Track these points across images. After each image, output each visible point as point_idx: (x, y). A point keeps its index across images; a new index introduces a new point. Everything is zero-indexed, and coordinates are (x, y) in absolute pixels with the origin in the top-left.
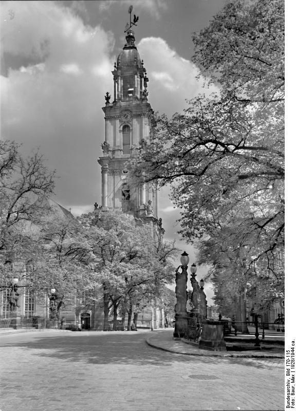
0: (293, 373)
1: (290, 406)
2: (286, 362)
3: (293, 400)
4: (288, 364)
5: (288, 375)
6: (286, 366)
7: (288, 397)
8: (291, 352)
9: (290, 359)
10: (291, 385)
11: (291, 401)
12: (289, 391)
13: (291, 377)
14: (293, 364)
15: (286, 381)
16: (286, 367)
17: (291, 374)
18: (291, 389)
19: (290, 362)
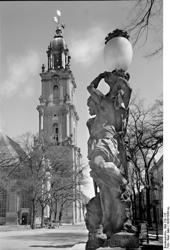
0: (168, 227)
1: (166, 247)
2: (164, 220)
3: (168, 243)
4: (165, 222)
5: (165, 228)
6: (164, 222)
7: (165, 241)
8: (167, 214)
9: (167, 218)
10: (167, 234)
11: (167, 244)
12: (166, 238)
13: (167, 229)
14: (168, 221)
15: (164, 232)
16: (164, 224)
17: (167, 227)
18: (167, 237)
19: (166, 220)
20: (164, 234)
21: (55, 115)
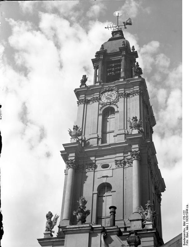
1: (185, 244)
4: (184, 219)
5: (184, 225)
7: (184, 238)
8: (186, 212)
9: (186, 216)
11: (186, 241)
12: (185, 235)
13: (186, 226)
14: (187, 219)
18: (186, 234)
19: (185, 218)
21: (105, 166)
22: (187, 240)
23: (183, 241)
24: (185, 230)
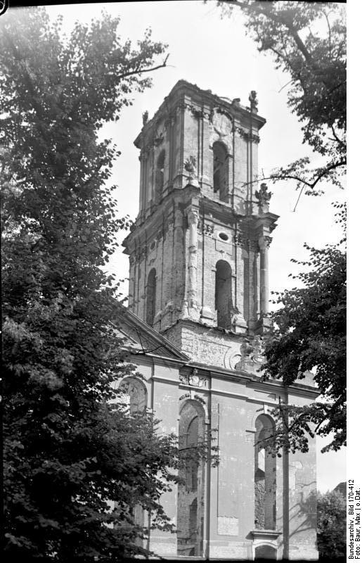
2: (348, 496)
4: (351, 499)
5: (351, 513)
6: (348, 499)
7: (352, 543)
10: (356, 527)
11: (355, 549)
12: (352, 536)
13: (355, 516)
15: (348, 523)
16: (348, 503)
17: (355, 512)
18: (355, 533)
20: (348, 526)
22: (358, 548)
23: (348, 549)
24: (352, 525)
